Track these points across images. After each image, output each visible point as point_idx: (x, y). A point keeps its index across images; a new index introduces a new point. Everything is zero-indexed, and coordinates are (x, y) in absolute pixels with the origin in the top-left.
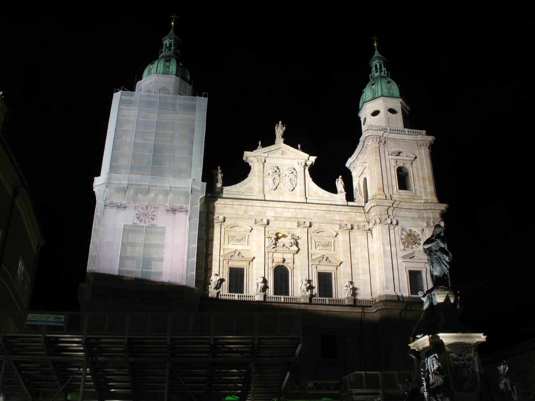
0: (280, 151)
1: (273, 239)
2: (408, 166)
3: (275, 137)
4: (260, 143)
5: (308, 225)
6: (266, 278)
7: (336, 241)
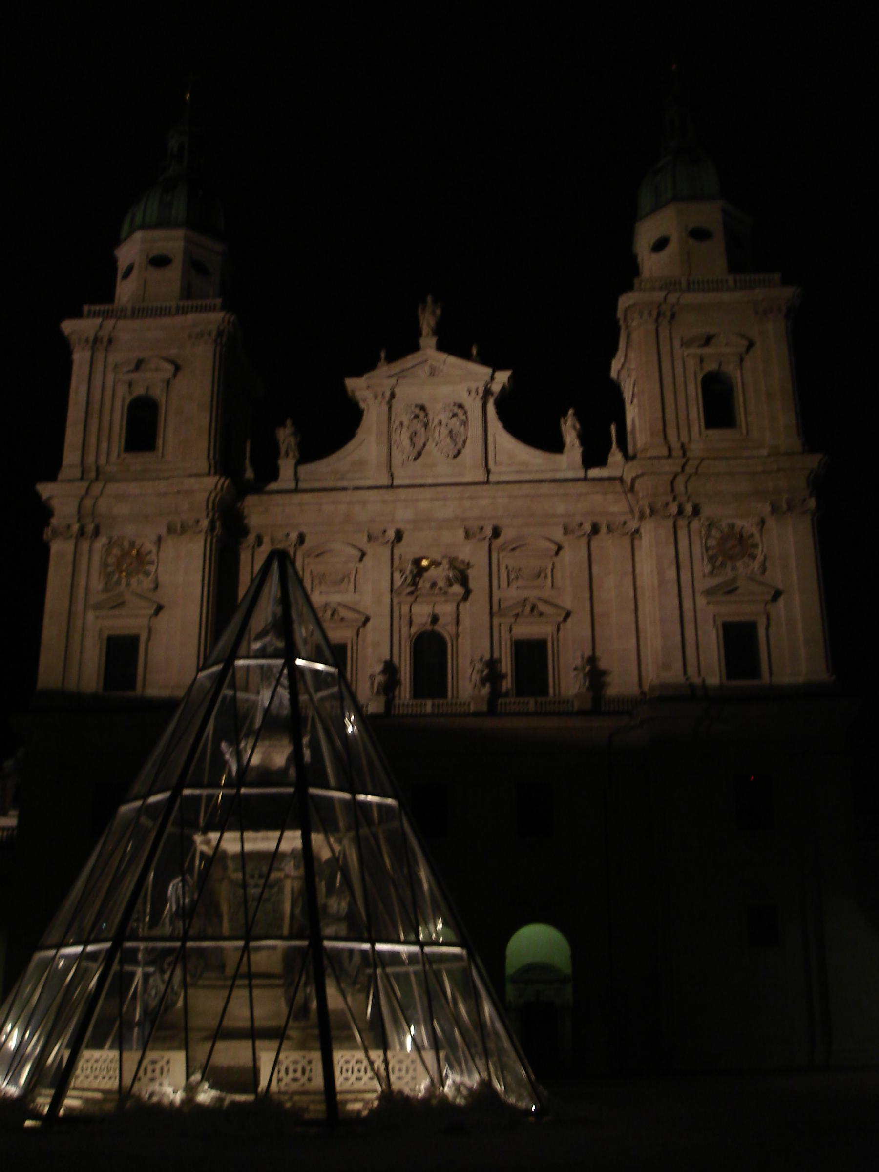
0: (427, 369)
1: (408, 572)
2: (731, 369)
3: (419, 334)
4: (383, 355)
5: (489, 532)
6: (396, 660)
7: (558, 566)
